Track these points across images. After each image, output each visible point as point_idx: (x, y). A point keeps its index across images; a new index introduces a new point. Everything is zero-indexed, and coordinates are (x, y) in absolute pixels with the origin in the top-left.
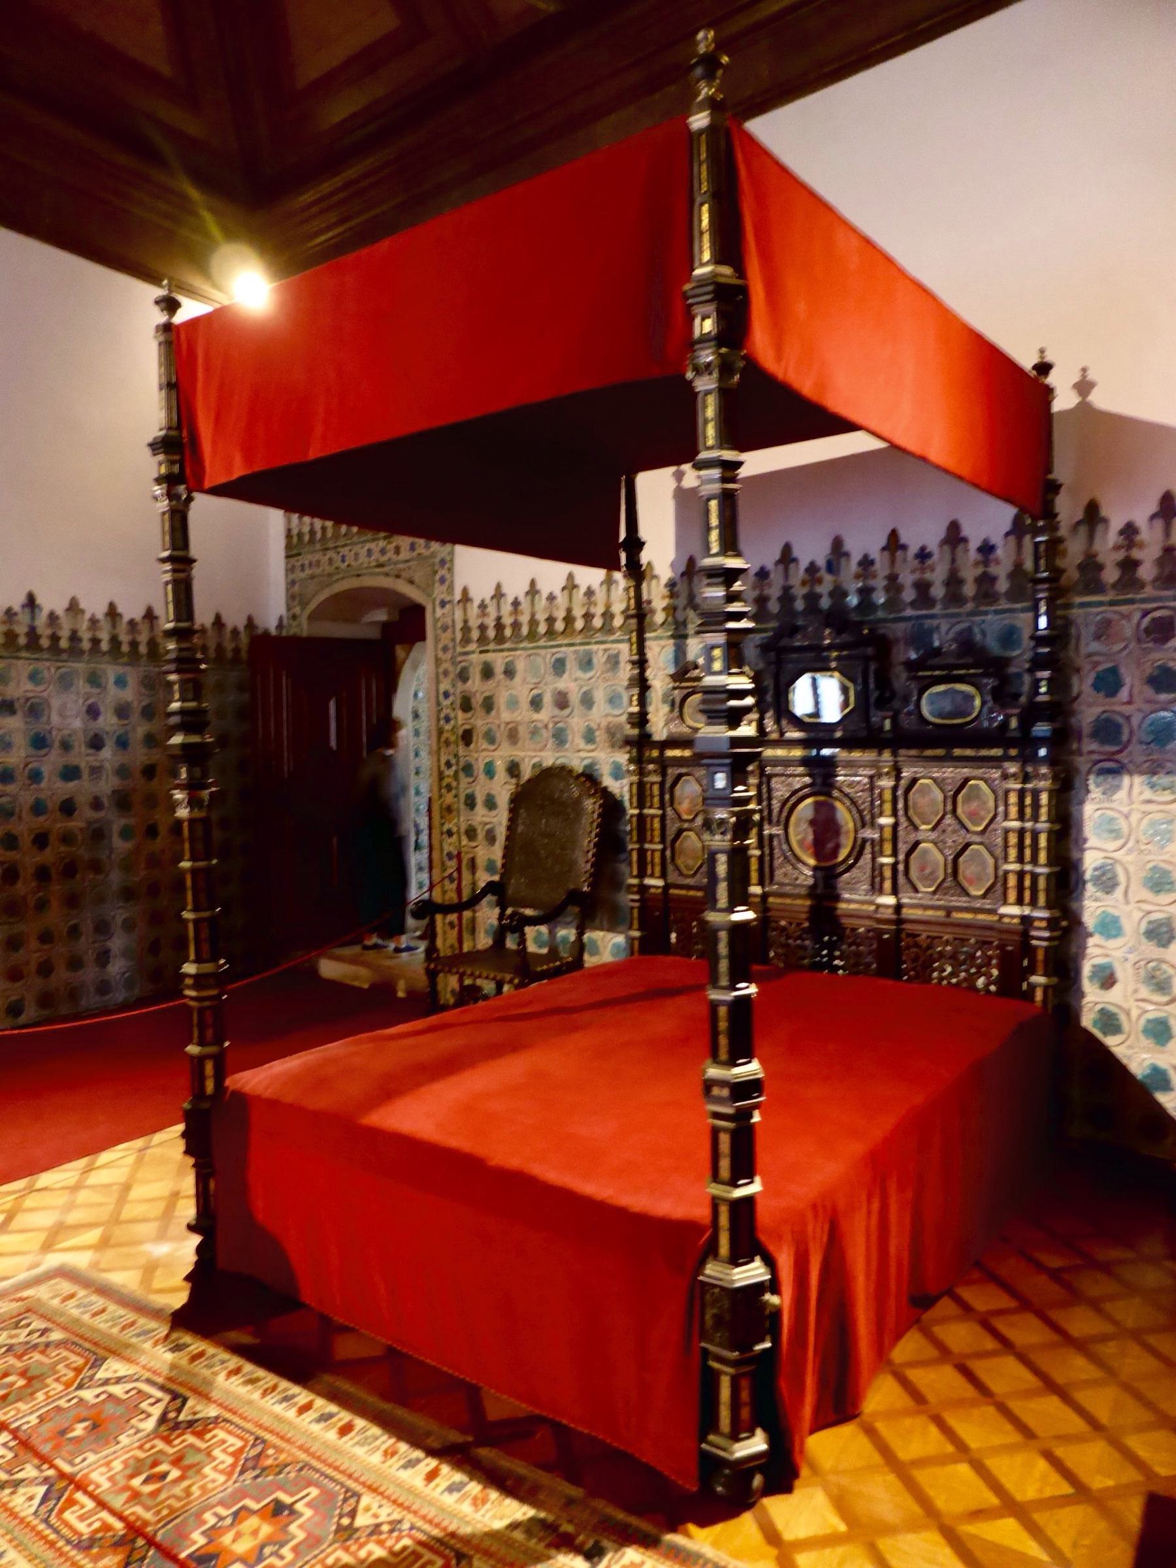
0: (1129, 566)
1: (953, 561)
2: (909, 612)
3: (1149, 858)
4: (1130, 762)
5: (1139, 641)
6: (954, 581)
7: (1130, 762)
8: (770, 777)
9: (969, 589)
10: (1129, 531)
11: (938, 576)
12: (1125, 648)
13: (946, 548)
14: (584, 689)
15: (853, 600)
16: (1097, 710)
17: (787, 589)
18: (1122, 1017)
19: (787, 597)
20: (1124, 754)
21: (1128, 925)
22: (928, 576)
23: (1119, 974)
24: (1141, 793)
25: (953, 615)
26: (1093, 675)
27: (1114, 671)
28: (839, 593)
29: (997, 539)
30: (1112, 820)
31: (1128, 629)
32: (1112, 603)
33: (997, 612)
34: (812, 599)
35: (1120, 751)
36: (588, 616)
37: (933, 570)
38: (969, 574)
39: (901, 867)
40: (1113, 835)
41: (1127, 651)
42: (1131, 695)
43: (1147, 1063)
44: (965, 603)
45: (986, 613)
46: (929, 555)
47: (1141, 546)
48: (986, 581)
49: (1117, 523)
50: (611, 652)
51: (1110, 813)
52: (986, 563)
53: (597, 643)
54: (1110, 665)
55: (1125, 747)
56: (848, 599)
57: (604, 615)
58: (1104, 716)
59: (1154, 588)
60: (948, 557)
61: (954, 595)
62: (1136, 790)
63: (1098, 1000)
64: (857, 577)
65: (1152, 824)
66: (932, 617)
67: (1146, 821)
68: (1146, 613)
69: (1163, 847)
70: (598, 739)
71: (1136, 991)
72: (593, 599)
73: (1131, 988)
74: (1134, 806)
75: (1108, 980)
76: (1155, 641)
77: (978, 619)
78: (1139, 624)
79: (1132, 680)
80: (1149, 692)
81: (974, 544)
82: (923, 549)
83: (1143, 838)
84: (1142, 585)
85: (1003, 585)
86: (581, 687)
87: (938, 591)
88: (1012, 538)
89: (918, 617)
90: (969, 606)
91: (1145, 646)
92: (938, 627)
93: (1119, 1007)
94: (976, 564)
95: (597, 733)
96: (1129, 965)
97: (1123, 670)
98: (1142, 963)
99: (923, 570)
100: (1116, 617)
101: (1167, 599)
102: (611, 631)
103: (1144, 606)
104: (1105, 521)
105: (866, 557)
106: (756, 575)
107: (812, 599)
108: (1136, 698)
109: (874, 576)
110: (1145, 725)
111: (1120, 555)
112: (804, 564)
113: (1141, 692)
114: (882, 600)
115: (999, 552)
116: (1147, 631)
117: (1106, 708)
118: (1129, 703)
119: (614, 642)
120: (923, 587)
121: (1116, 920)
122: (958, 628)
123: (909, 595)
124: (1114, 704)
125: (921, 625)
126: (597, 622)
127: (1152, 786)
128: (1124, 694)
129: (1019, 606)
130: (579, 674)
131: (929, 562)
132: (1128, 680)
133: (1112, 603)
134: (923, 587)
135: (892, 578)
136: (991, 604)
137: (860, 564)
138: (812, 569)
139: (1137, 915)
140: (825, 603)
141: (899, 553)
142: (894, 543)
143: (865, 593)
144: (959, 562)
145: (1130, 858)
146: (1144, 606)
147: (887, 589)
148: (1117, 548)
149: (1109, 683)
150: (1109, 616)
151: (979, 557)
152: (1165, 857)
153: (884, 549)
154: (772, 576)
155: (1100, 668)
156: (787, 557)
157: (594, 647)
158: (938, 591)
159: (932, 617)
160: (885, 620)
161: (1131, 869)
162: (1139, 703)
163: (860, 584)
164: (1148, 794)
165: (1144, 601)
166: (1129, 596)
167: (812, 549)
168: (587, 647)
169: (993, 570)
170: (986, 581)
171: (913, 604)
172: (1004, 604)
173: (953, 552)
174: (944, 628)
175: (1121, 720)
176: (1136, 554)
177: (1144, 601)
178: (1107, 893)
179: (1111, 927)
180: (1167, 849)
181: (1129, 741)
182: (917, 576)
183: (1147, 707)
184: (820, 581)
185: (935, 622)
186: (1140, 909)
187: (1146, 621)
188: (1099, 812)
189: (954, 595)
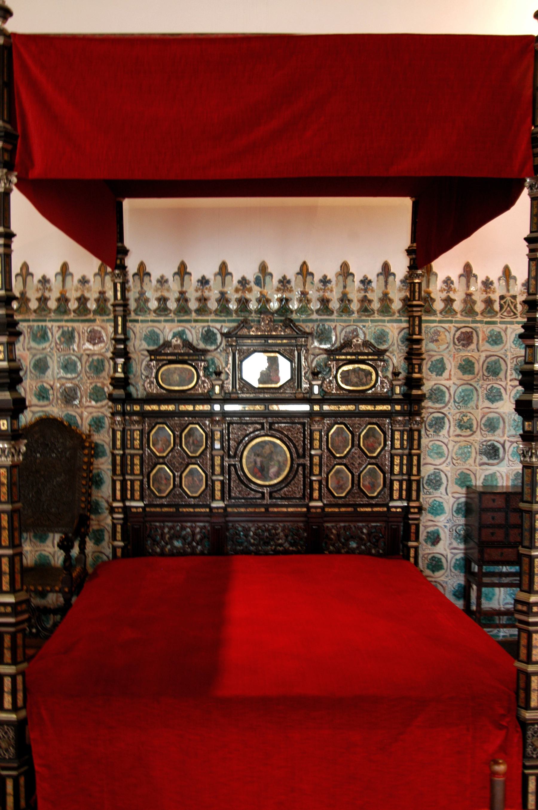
0: (449, 301)
1: (345, 287)
2: (315, 316)
3: (459, 467)
4: (449, 413)
5: (454, 343)
6: (344, 299)
7: (449, 413)
8: (229, 424)
9: (355, 306)
10: (448, 281)
11: (334, 296)
12: (447, 347)
13: (341, 278)
14: (38, 357)
15: (274, 305)
16: (433, 383)
17: (223, 294)
18: (443, 560)
19: (223, 299)
20: (447, 408)
21: (447, 507)
22: (328, 295)
23: (442, 536)
24: (454, 431)
25: (345, 321)
26: (430, 363)
27: (441, 361)
28: (264, 300)
29: (372, 276)
30: (439, 447)
31: (449, 337)
32: (440, 322)
33: (372, 321)
34: (243, 303)
35: (444, 407)
36: (43, 300)
37: (332, 291)
38: (355, 296)
39: (324, 483)
40: (440, 455)
41: (448, 350)
42: (450, 375)
43: (455, 585)
44: (353, 313)
45: (366, 321)
46: (330, 281)
47: (455, 291)
48: (365, 300)
49: (441, 277)
50: (66, 329)
51: (437, 443)
52: (366, 290)
53: (50, 321)
54: (438, 357)
55: (446, 405)
56: (271, 304)
57: (58, 300)
58: (435, 387)
59: (462, 315)
60: (341, 285)
61: (345, 310)
62: (452, 428)
63: (431, 552)
64: (278, 290)
65: (460, 448)
66: (333, 321)
67: (457, 447)
68: (458, 329)
69: (465, 462)
70: (51, 397)
71: (450, 544)
72: (48, 286)
73: (448, 542)
74: (450, 439)
75: (435, 539)
76: (463, 345)
77: (360, 325)
78: (455, 334)
79: (451, 365)
80: (460, 374)
81: (358, 278)
82: (325, 277)
83: (455, 457)
84: (456, 313)
85: (376, 305)
86: (34, 355)
87: (335, 305)
88: (382, 278)
89: (321, 320)
90: (355, 316)
91: (457, 347)
92: (335, 328)
93: (442, 555)
94: (359, 290)
95: (51, 392)
96: (447, 530)
97: (446, 361)
98: (454, 528)
99: (325, 291)
100: (443, 330)
101: (468, 322)
102: (66, 311)
103: (457, 325)
104: (436, 275)
105: (284, 277)
106: (198, 281)
107: (243, 303)
108: (452, 377)
109: (291, 291)
110: (458, 392)
111: (444, 295)
112: (236, 278)
113: (455, 374)
114: (296, 307)
115: (374, 285)
116: (458, 339)
117: (436, 382)
118: (450, 379)
119: (67, 321)
120: (325, 302)
121: (440, 505)
122: (348, 329)
123: (315, 305)
124: (440, 380)
125: (323, 325)
126: (52, 304)
127: (461, 427)
128: (446, 374)
129: (387, 318)
130: (33, 344)
131: (329, 286)
132: (448, 366)
133: (440, 322)
134: (325, 302)
135: (304, 294)
136: (369, 316)
137: (280, 281)
138: (243, 282)
139: (452, 500)
140: (253, 306)
141: (309, 278)
142: (304, 271)
143: (284, 302)
144: (347, 289)
145: (448, 468)
146: (457, 325)
147: (300, 301)
148: (442, 291)
149: (439, 368)
150: (439, 329)
151: (362, 286)
152: (467, 467)
153: (298, 274)
154: (211, 283)
155: (434, 359)
156: (223, 271)
157: (49, 324)
158: (335, 305)
159: (333, 321)
160: (298, 321)
161: (449, 475)
162: (454, 379)
163: (280, 295)
164: (458, 431)
165: (456, 322)
166: (450, 318)
167: (243, 268)
168: (44, 324)
169: (370, 295)
170: (365, 300)
171: (317, 311)
172: (377, 317)
173: (345, 281)
174: (339, 329)
175: (445, 389)
176: (452, 295)
177: (456, 322)
178: (436, 489)
179: (437, 510)
180: (467, 462)
181: (449, 402)
182: (321, 293)
183: (459, 382)
184: (250, 290)
185: (333, 325)
186: (453, 497)
187: (458, 333)
188: (431, 444)
189: (345, 310)
